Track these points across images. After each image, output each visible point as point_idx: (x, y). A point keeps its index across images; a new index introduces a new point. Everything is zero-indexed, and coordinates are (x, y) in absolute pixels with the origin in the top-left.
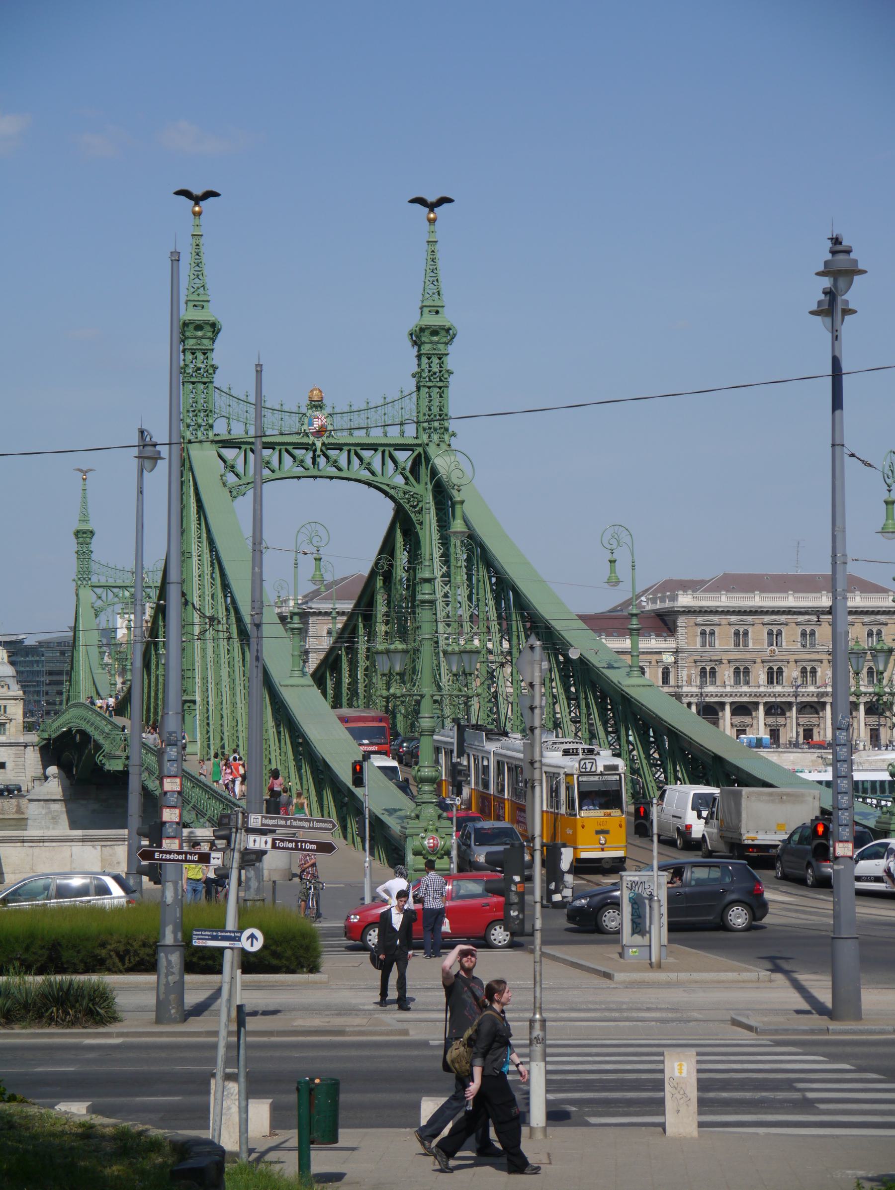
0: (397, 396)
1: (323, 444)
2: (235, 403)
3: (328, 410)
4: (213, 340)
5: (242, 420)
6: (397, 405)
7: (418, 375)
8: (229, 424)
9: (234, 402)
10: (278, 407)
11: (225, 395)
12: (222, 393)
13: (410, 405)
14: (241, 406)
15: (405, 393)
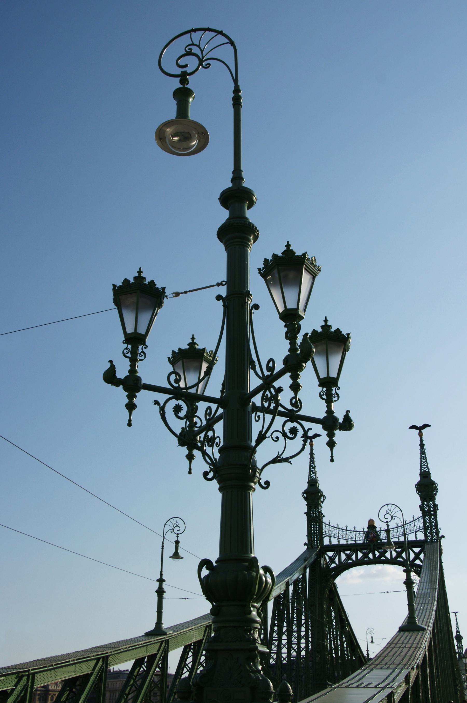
0: (412, 519)
1: (374, 545)
2: (332, 529)
3: (378, 529)
4: (322, 502)
5: (336, 537)
6: (412, 525)
7: (422, 508)
8: (330, 539)
9: (332, 530)
10: (353, 530)
11: (327, 526)
12: (326, 525)
13: (420, 523)
14: (336, 530)
15: (415, 518)
